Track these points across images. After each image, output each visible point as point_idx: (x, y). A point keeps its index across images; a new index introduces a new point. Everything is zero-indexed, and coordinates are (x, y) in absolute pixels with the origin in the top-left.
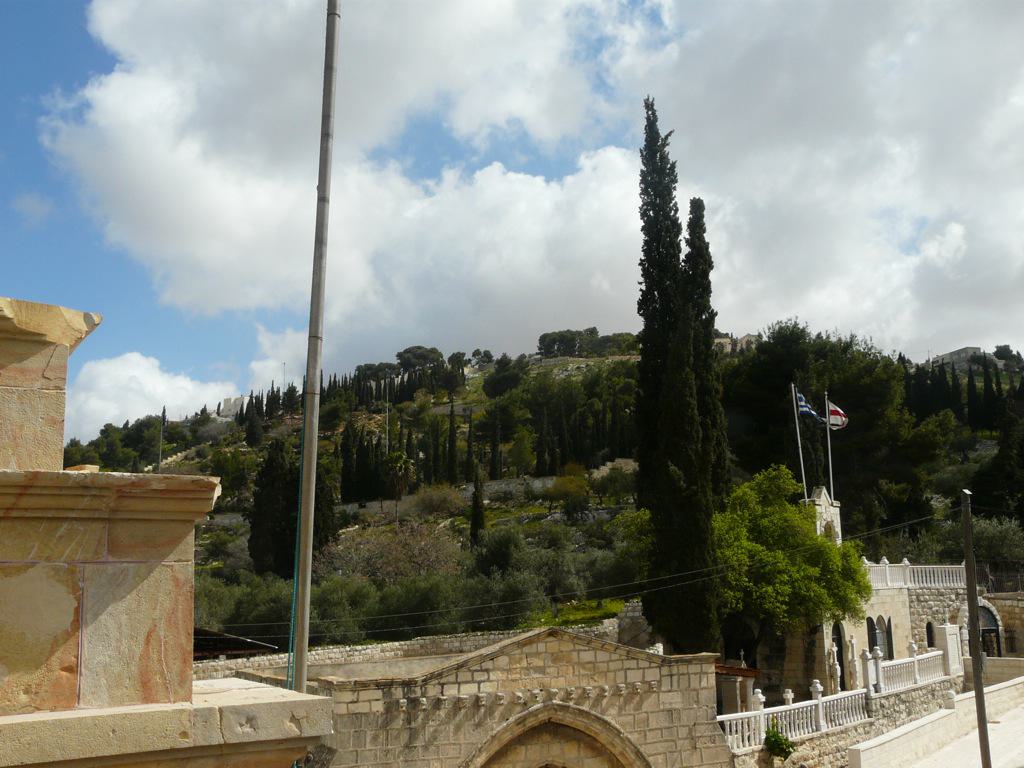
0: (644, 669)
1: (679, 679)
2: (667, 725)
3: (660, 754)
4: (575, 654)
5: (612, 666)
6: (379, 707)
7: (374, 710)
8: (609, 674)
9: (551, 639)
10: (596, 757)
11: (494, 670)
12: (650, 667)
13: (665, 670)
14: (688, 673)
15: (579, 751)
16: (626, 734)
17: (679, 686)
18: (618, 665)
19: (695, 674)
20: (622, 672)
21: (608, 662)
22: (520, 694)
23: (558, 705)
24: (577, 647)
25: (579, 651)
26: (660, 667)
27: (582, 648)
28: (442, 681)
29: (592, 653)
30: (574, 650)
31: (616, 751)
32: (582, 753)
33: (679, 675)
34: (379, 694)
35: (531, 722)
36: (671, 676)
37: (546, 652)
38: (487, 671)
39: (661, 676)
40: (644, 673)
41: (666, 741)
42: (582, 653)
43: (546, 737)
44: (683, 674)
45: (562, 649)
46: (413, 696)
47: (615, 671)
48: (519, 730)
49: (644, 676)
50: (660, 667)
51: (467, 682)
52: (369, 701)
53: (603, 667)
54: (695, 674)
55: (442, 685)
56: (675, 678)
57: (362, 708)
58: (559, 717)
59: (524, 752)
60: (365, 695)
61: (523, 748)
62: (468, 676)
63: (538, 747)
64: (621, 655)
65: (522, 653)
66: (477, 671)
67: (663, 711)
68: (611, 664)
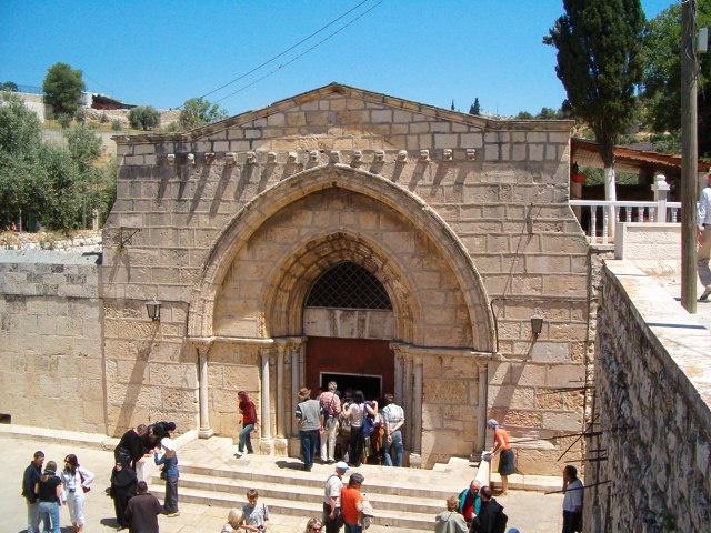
0: (460, 133)
1: (511, 151)
2: (490, 202)
3: (476, 235)
4: (366, 113)
5: (415, 128)
6: (151, 161)
7: (147, 163)
8: (410, 137)
9: (337, 96)
10: (399, 231)
11: (268, 127)
12: (469, 132)
13: (491, 137)
14: (528, 144)
15: (378, 223)
16: (427, 209)
17: (511, 156)
18: (425, 127)
19: (537, 144)
20: (429, 137)
21: (409, 124)
22: (294, 154)
23: (341, 168)
24: (369, 105)
25: (371, 110)
26: (483, 133)
27: (376, 107)
28: (213, 138)
29: (389, 113)
30: (365, 109)
31: (420, 225)
32: (382, 226)
33: (513, 144)
34: (152, 148)
35: (308, 187)
36: (500, 144)
37: (330, 110)
38: (260, 128)
39: (485, 143)
40: (459, 138)
41: (487, 221)
42: (375, 114)
43: (338, 204)
44: (518, 143)
45: (352, 107)
46: (183, 151)
47: (418, 135)
48: (296, 194)
49: (459, 143)
50: (483, 133)
51: (238, 140)
52: (143, 155)
53: (403, 129)
54: (537, 144)
55: (212, 142)
56: (506, 148)
57: (138, 161)
58: (342, 182)
59: (310, 219)
60: (140, 149)
61: (310, 214)
62: (239, 134)
63: (327, 214)
64: (426, 117)
65: (301, 110)
66: (247, 128)
67: (485, 185)
68: (412, 125)
